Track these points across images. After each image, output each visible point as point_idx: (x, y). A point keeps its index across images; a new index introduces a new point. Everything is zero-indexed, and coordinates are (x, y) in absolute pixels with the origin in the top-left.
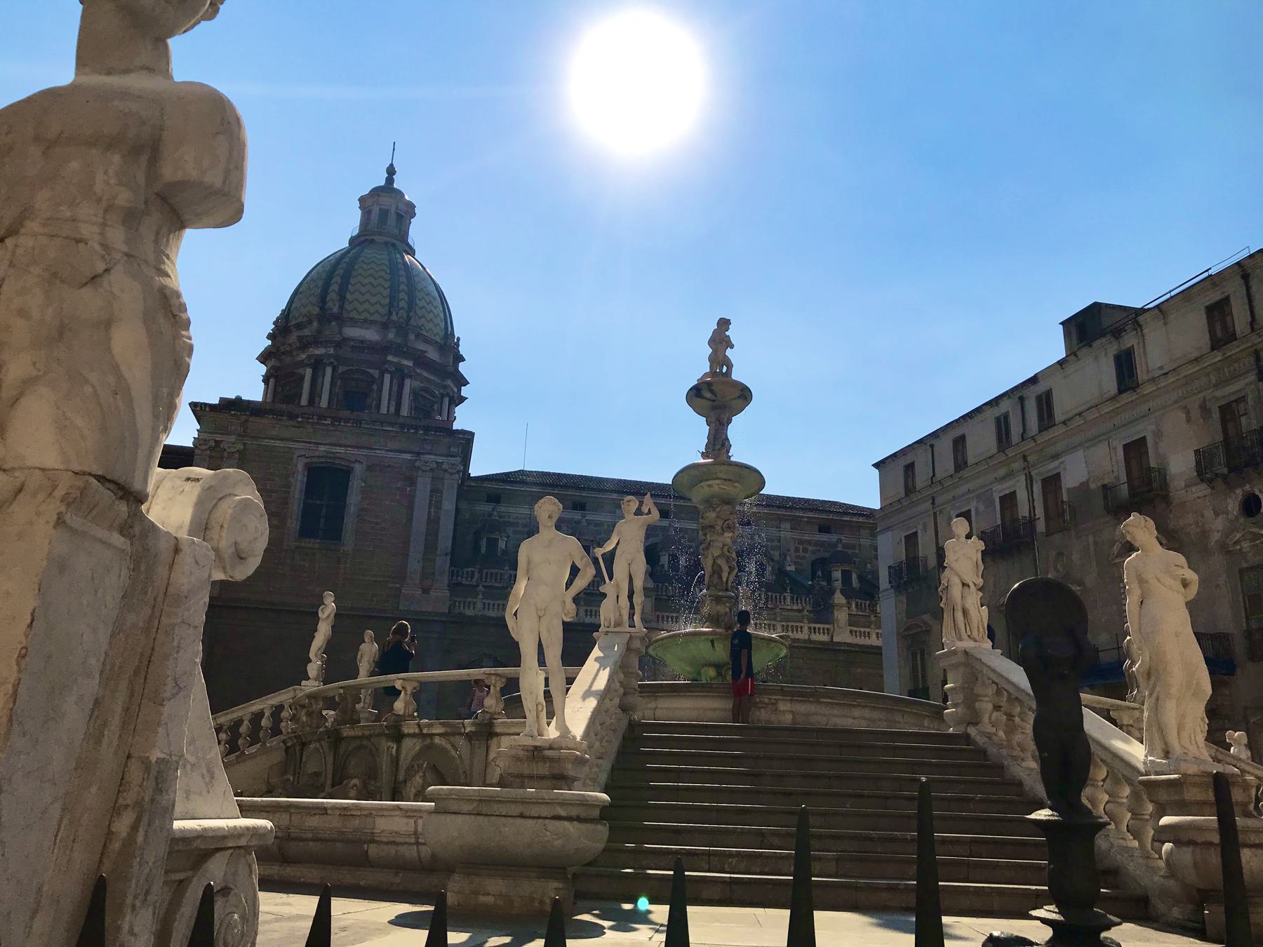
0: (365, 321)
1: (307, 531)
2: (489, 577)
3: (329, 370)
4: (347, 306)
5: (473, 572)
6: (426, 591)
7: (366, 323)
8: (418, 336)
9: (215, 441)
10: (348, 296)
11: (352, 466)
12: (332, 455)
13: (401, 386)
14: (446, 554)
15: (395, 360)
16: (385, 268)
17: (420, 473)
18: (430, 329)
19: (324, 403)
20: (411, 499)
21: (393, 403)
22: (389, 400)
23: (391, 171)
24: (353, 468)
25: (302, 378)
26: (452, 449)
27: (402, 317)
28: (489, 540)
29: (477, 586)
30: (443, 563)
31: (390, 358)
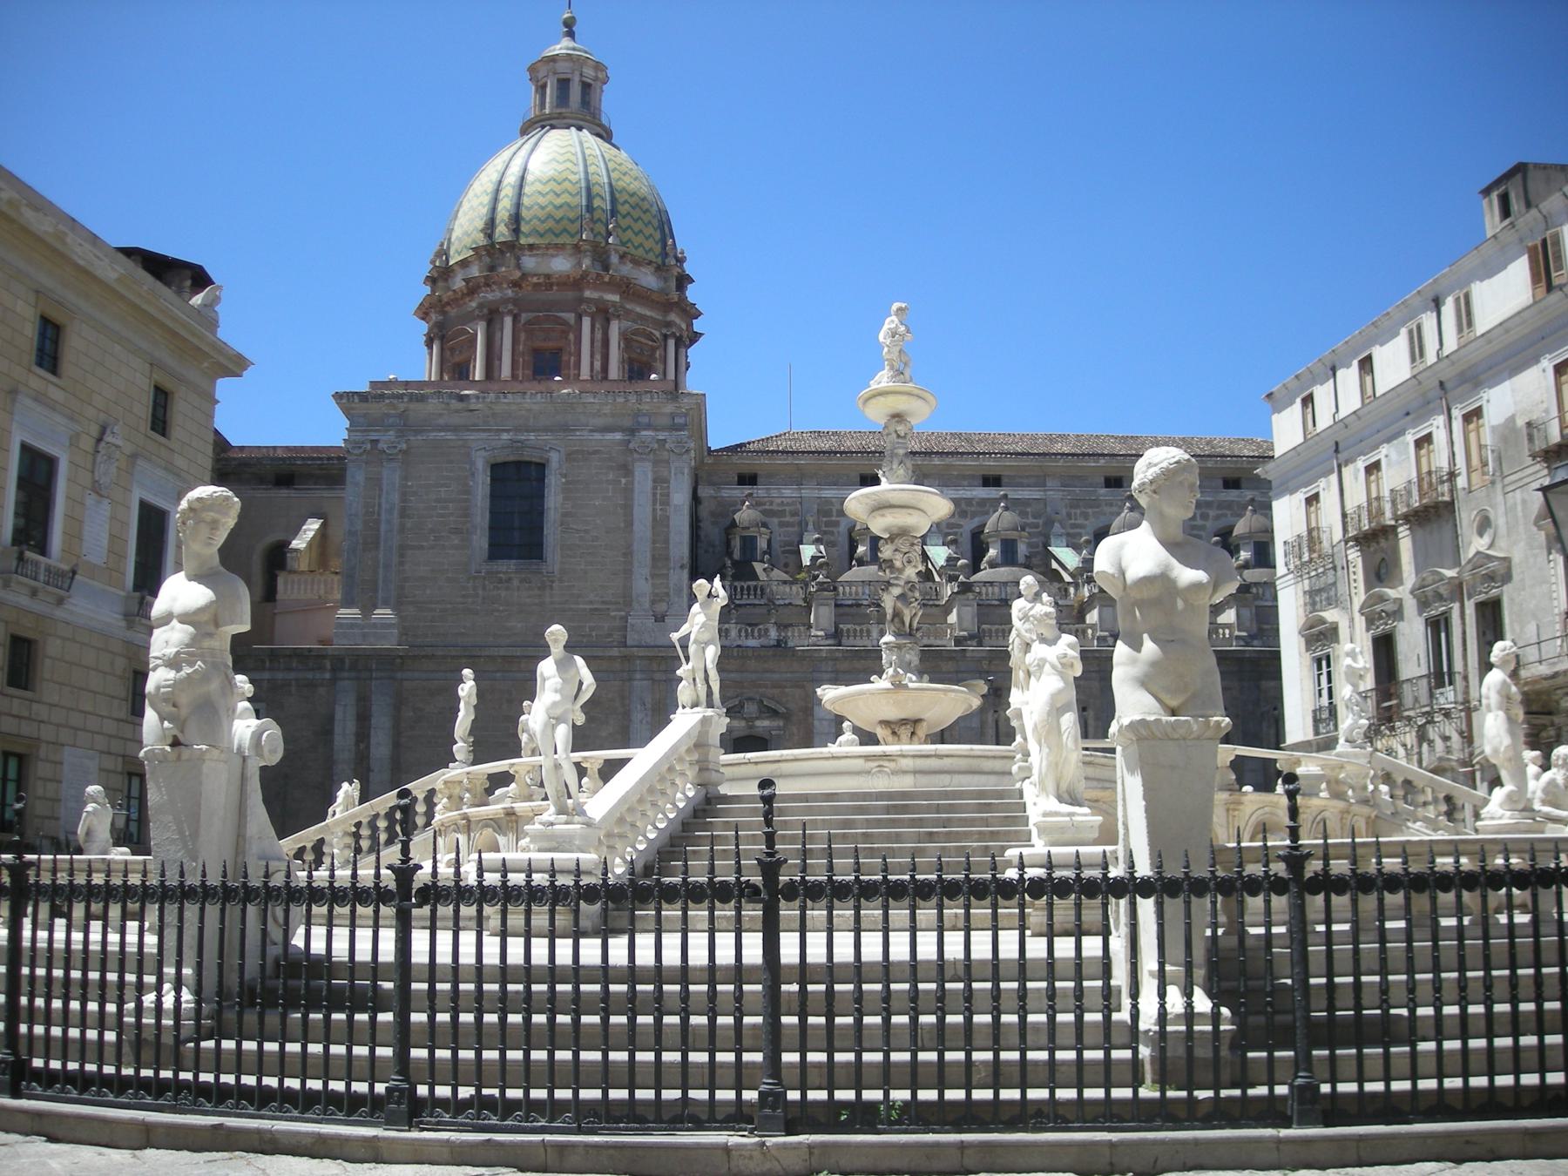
1: (497, 551)
3: (508, 321)
9: (372, 441)
14: (682, 567)
18: (641, 245)
20: (628, 492)
21: (598, 357)
22: (592, 356)
24: (548, 460)
27: (599, 233)
28: (744, 539)
31: (588, 294)
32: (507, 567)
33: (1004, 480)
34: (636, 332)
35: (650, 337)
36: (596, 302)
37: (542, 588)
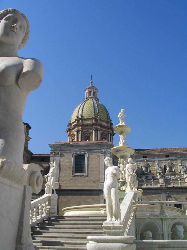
3: (80, 132)
8: (101, 120)
15: (95, 127)
16: (91, 105)
19: (80, 140)
20: (100, 160)
21: (96, 137)
26: (108, 147)
27: (96, 116)
34: (103, 133)
35: (105, 134)
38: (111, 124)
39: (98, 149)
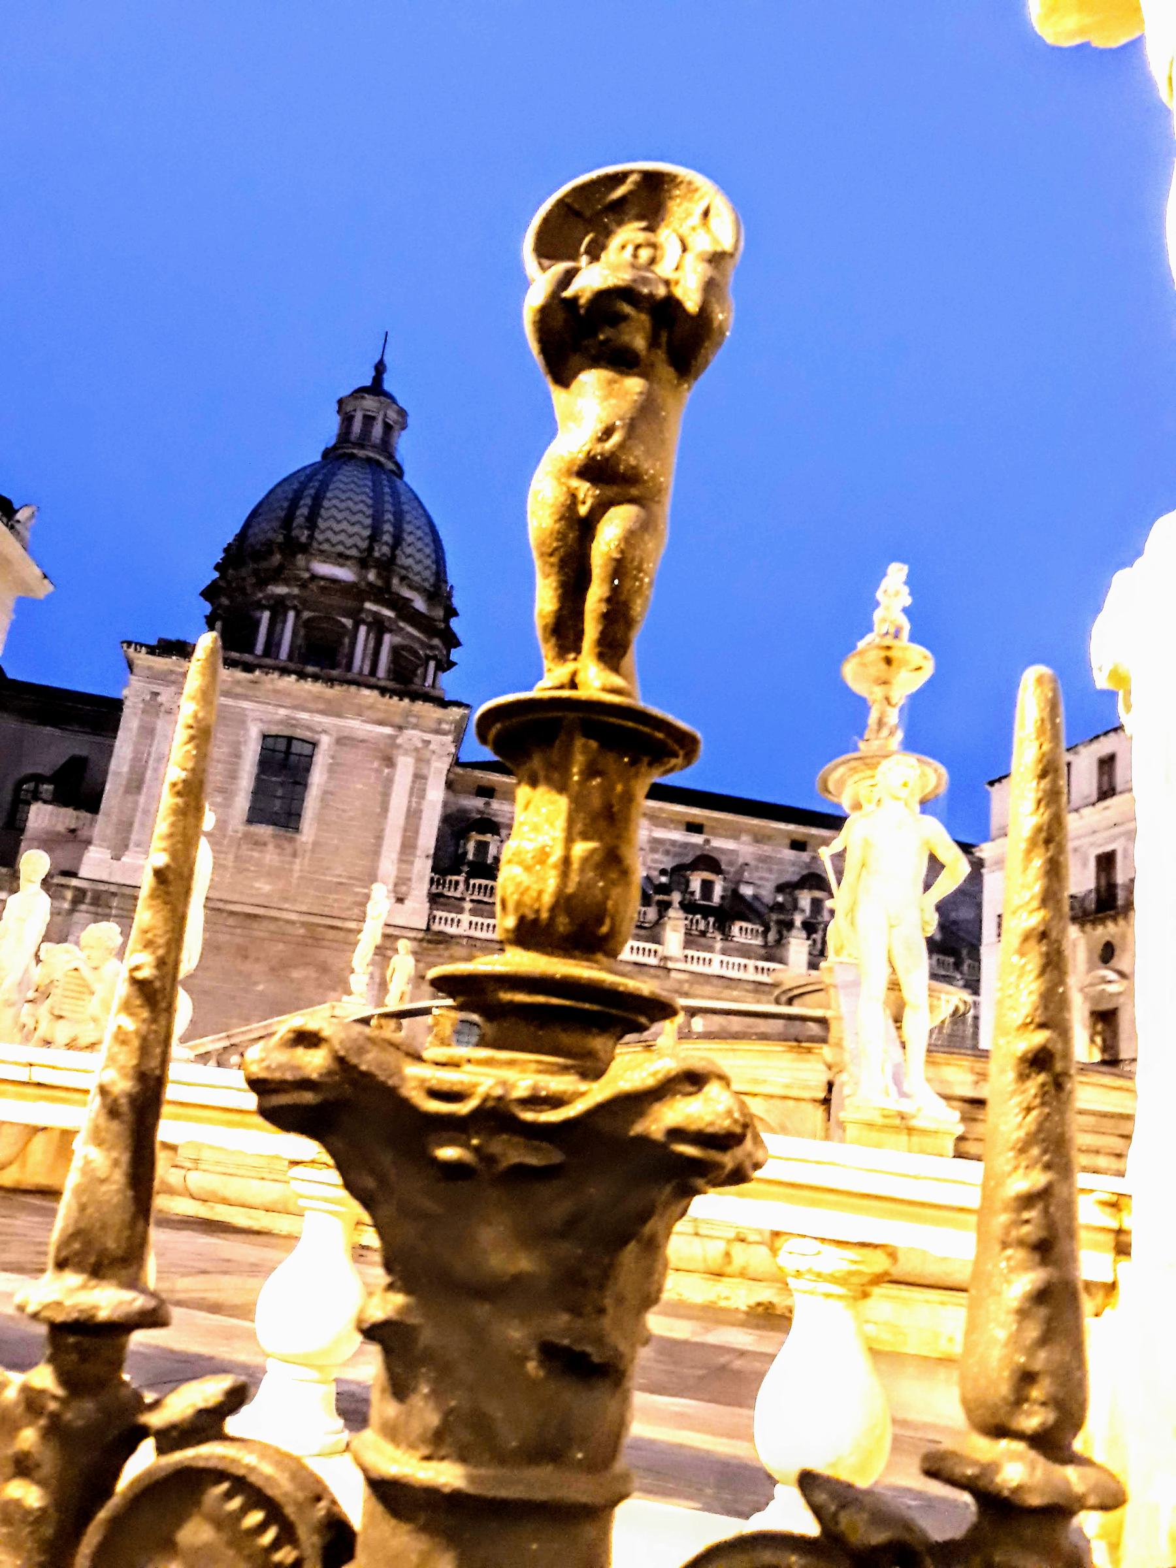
0: (340, 555)
1: (256, 815)
2: (477, 890)
3: (291, 615)
4: (319, 537)
5: (457, 883)
6: (400, 900)
7: (341, 559)
10: (322, 524)
11: (317, 737)
12: (294, 722)
13: (379, 643)
14: (427, 856)
17: (401, 751)
20: (389, 782)
21: (368, 663)
23: (380, 368)
25: (258, 623)
29: (463, 899)
30: (423, 867)
32: (264, 831)
33: (705, 829)
34: (403, 647)
35: (415, 653)
36: (376, 614)
37: (295, 855)
38: (452, 612)
39: (392, 726)
